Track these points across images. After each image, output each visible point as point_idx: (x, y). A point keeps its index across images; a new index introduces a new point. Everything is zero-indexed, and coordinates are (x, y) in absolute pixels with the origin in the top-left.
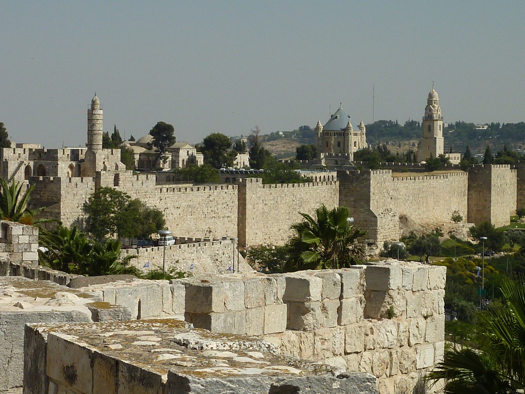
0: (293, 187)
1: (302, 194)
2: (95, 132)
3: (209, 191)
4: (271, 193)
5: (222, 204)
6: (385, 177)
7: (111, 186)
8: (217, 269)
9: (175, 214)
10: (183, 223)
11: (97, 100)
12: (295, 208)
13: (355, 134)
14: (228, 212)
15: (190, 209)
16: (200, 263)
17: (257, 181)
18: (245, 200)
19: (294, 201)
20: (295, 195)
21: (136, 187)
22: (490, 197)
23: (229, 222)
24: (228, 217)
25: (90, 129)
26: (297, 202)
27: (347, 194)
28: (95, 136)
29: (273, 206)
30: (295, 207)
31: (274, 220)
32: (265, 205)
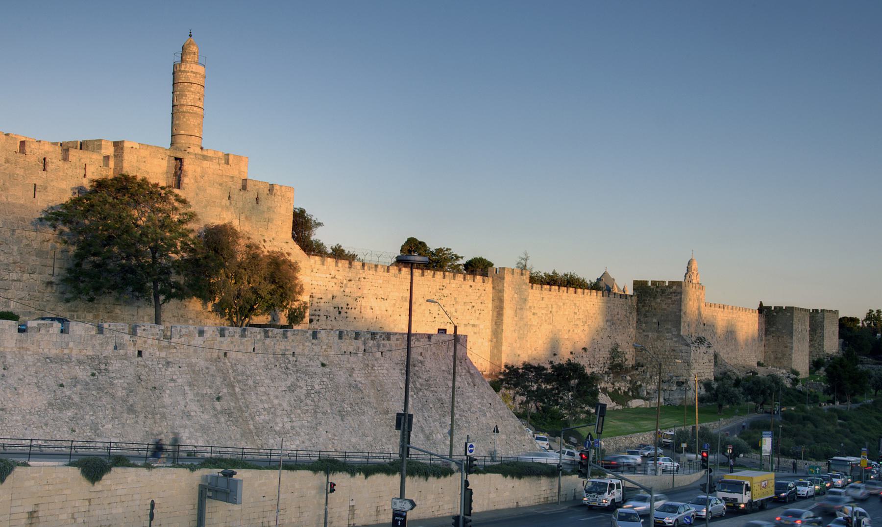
2: (185, 108)
3: (442, 280)
4: (543, 298)
5: (465, 303)
8: (415, 396)
9: (377, 308)
11: (192, 47)
12: (577, 325)
14: (473, 318)
17: (522, 274)
19: (575, 313)
20: (577, 305)
23: (475, 333)
24: (474, 326)
26: (581, 316)
28: (184, 117)
29: (545, 318)
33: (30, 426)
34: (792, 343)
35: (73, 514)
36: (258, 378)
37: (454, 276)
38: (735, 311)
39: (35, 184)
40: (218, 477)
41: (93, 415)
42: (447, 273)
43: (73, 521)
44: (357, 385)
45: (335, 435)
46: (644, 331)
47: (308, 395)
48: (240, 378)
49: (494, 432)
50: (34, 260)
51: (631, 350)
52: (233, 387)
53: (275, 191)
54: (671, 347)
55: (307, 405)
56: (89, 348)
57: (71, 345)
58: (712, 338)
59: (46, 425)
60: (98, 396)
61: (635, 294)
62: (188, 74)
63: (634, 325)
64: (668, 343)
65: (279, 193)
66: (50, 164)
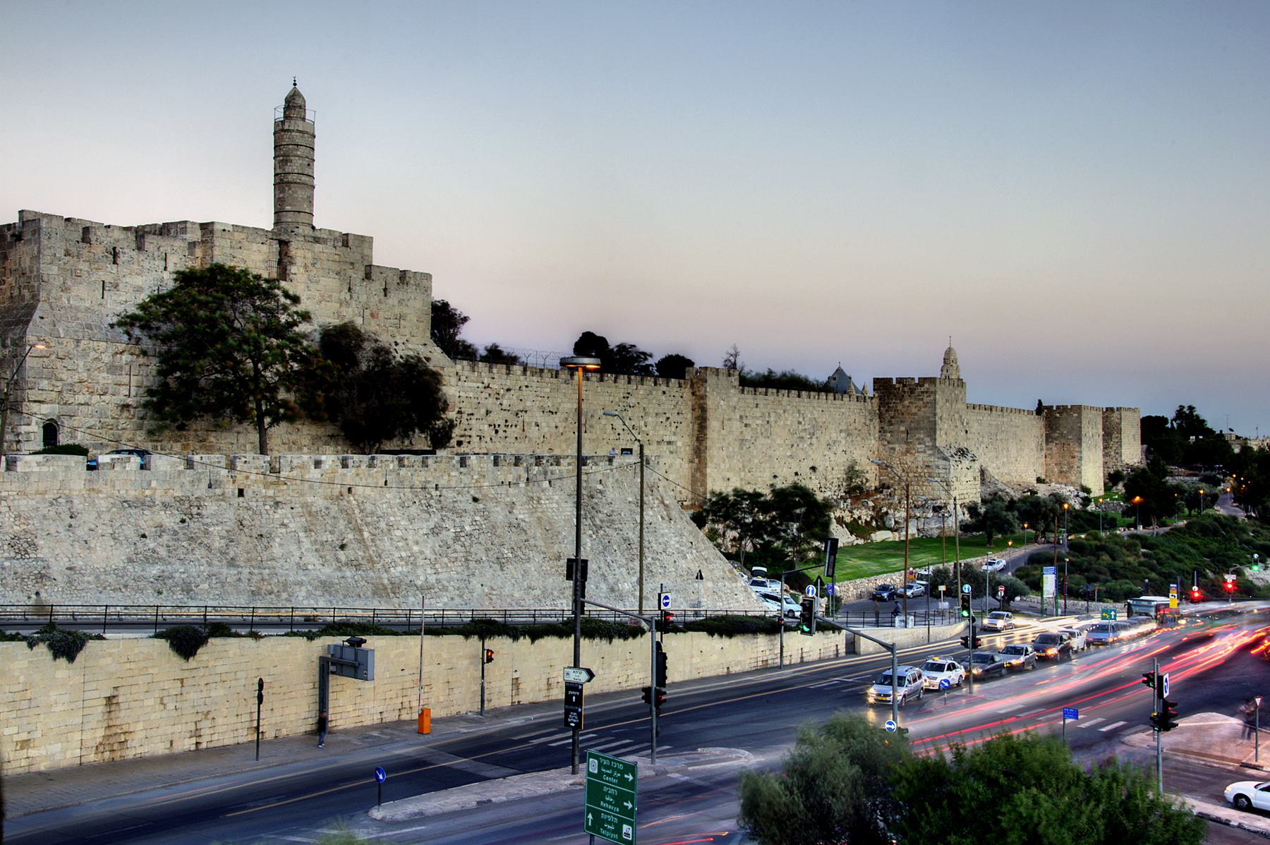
0: (799, 396)
4: (757, 405)
5: (657, 414)
6: (957, 392)
8: (594, 536)
9: (544, 424)
12: (803, 438)
14: (669, 433)
16: (535, 515)
17: (729, 375)
18: (703, 409)
19: (800, 423)
21: (363, 298)
22: (1081, 452)
23: (671, 452)
24: (669, 443)
25: (279, 171)
26: (807, 427)
28: (290, 189)
29: (761, 430)
30: (803, 434)
31: (763, 457)
32: (746, 425)
33: (105, 588)
35: (162, 699)
36: (392, 519)
37: (642, 380)
38: (1005, 414)
39: (103, 281)
40: (342, 647)
41: (184, 573)
42: (633, 377)
43: (162, 706)
44: (519, 524)
45: (492, 589)
46: (889, 443)
47: (457, 538)
48: (369, 519)
49: (697, 578)
50: (104, 378)
52: (361, 531)
53: (408, 279)
54: (924, 462)
55: (455, 551)
56: (177, 487)
57: (154, 484)
58: (978, 448)
59: (126, 586)
60: (190, 548)
61: (877, 395)
62: (293, 134)
63: (877, 435)
64: (921, 458)
65: (412, 282)
66: (121, 255)
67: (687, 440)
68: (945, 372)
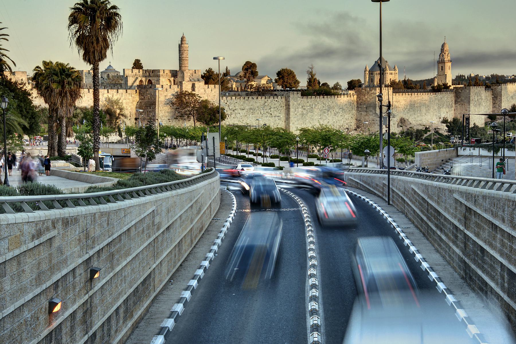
0: (323, 98)
1: (330, 103)
2: (183, 58)
7: (190, 91)
9: (241, 113)
10: (247, 119)
12: (325, 112)
13: (391, 74)
15: (252, 111)
17: (298, 94)
18: (289, 105)
19: (324, 107)
21: (207, 92)
23: (279, 119)
24: (278, 116)
26: (326, 108)
27: (361, 104)
30: (325, 111)
34: (469, 108)
37: (269, 97)
46: (360, 112)
50: (167, 114)
51: (354, 121)
54: (372, 119)
58: (404, 111)
64: (371, 117)
67: (284, 115)
68: (441, 57)
